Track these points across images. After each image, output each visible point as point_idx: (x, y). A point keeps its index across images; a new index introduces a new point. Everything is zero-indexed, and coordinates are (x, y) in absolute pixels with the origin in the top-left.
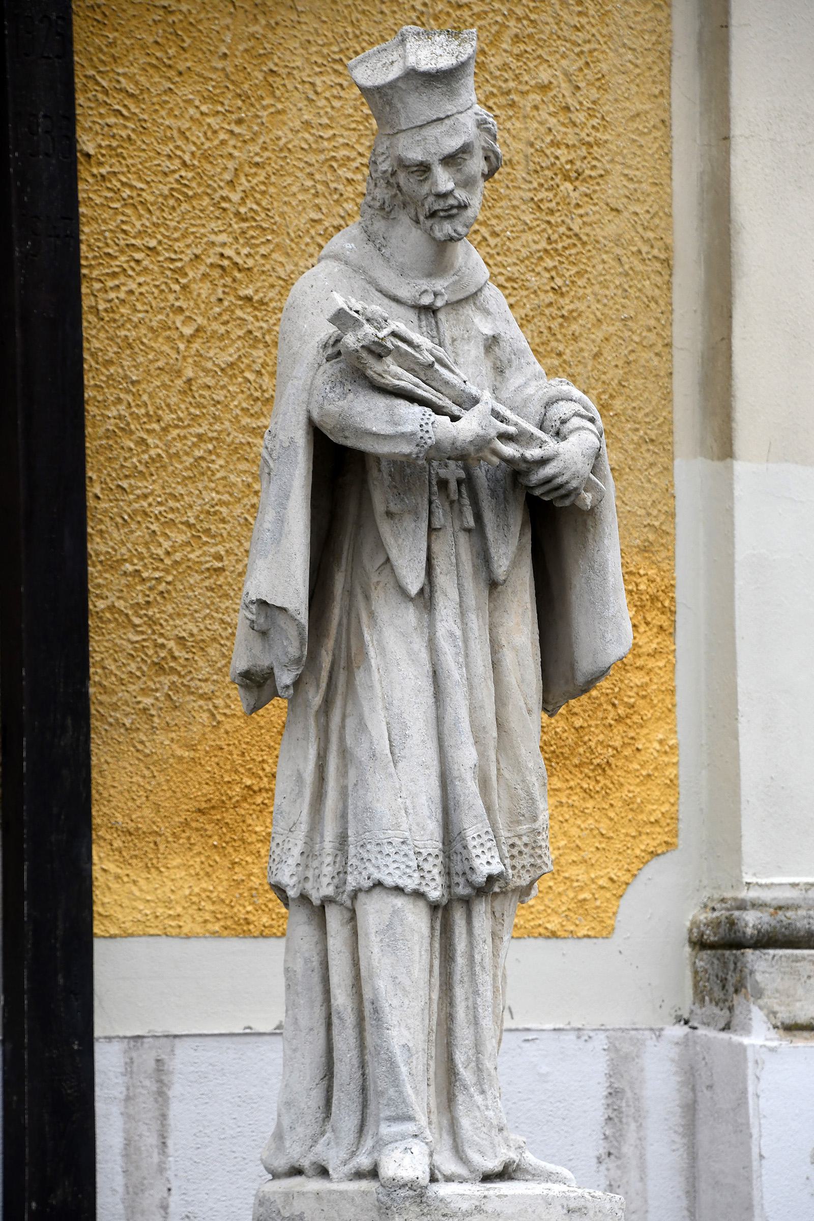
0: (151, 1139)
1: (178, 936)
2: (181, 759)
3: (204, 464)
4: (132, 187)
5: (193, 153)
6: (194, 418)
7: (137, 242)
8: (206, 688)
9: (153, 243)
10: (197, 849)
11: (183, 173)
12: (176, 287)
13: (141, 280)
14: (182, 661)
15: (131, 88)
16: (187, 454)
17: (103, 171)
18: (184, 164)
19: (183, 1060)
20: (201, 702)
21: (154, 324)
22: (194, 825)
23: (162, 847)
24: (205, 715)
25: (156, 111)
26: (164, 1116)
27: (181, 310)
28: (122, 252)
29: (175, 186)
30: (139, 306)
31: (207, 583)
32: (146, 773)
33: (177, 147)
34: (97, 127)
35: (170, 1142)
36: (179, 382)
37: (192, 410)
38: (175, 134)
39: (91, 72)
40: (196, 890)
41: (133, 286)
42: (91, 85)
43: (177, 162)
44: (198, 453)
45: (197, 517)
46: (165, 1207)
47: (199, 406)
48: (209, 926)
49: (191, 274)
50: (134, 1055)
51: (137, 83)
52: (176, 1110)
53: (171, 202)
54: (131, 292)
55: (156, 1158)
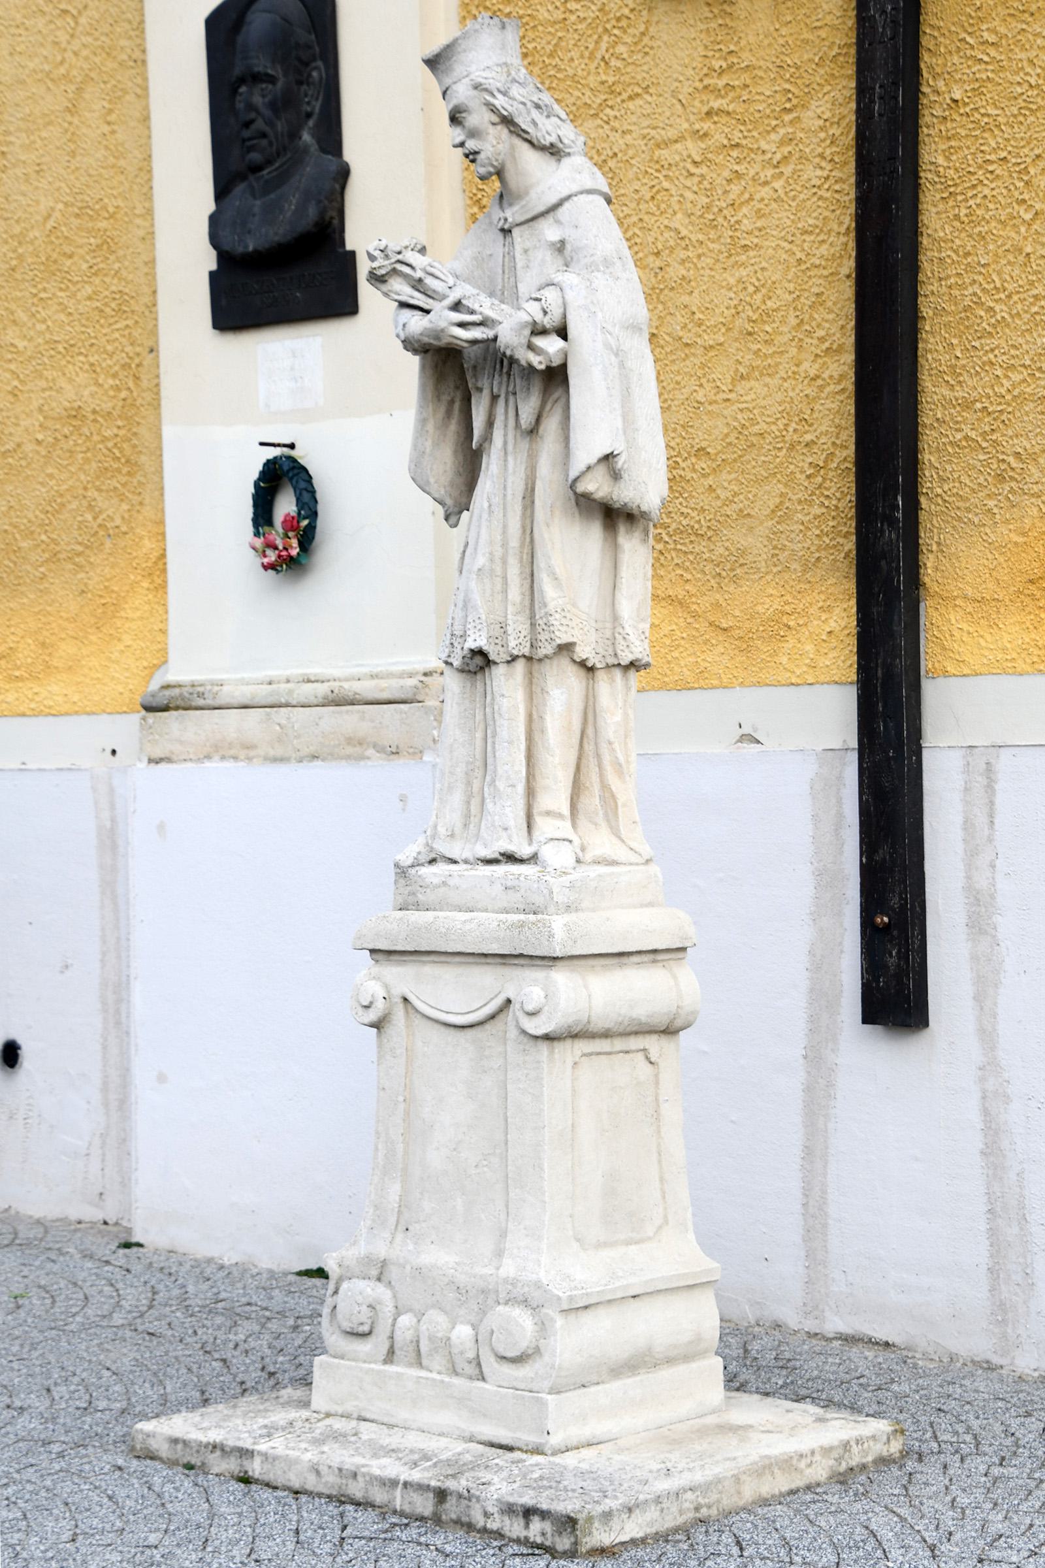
0: (981, 820)
1: (1014, 674)
2: (1016, 543)
3: (1038, 318)
4: (988, 115)
5: (1038, 75)
6: (1032, 283)
7: (993, 157)
8: (1036, 488)
9: (1003, 154)
10: (1028, 609)
11: (1029, 93)
12: (1022, 184)
13: (993, 185)
14: (1018, 471)
15: (992, 38)
16: (1026, 312)
17: (967, 110)
18: (1031, 86)
19: (1004, 762)
20: (1033, 500)
21: (1003, 218)
22: (1026, 592)
23: (1002, 610)
24: (1035, 510)
25: (1011, 50)
26: (992, 803)
27: (1024, 201)
28: (980, 167)
29: (1023, 104)
30: (991, 206)
31: (1039, 409)
32: (990, 556)
33: (1027, 74)
34: (965, 77)
35: (996, 821)
36: (1021, 258)
37: (1030, 277)
38: (1025, 63)
39: (964, 35)
40: (1027, 640)
41: (986, 191)
42: (961, 45)
43: (1026, 86)
44: (1035, 309)
45: (1032, 360)
46: (993, 867)
47: (1036, 273)
48: (1036, 666)
49: (1032, 172)
50: (970, 759)
51: (996, 33)
52: (999, 800)
53: (1021, 118)
54: (985, 196)
55: (986, 832)
